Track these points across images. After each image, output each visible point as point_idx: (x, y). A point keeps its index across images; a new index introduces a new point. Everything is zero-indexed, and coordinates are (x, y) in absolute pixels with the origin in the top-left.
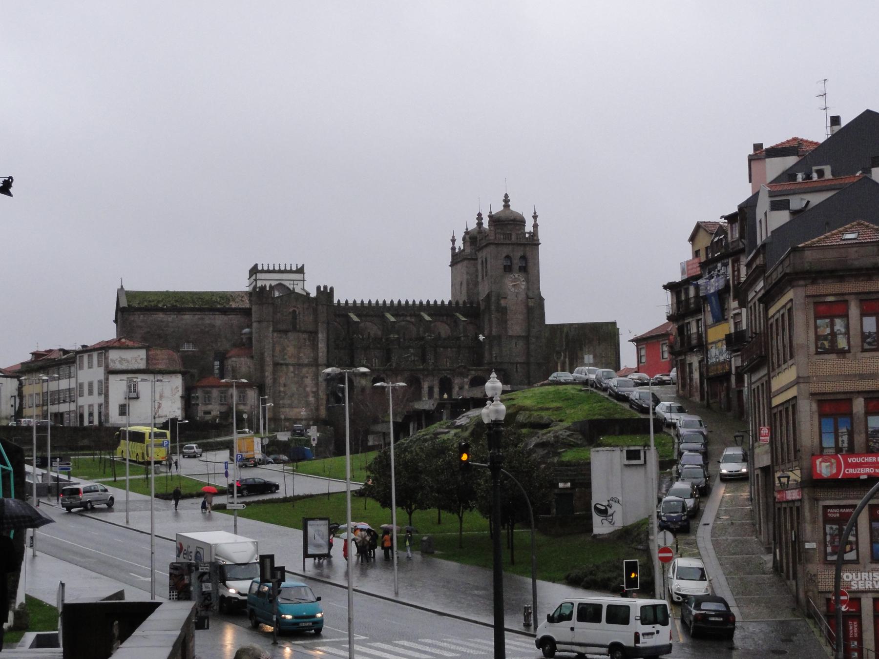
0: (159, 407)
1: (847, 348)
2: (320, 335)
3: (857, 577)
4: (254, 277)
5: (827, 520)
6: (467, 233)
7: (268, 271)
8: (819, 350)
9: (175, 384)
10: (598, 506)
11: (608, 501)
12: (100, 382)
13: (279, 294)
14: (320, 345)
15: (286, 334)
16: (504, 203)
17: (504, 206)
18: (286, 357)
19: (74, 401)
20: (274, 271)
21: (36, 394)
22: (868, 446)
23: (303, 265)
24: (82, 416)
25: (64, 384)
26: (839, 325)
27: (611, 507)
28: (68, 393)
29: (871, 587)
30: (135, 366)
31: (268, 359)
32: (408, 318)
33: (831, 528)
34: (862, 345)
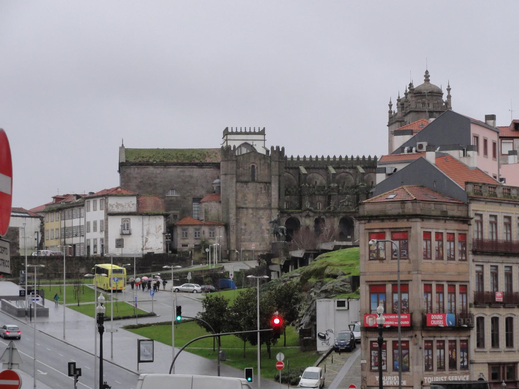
0: (146, 242)
1: (384, 258)
2: (273, 185)
3: (386, 379)
4: (225, 138)
5: (372, 348)
6: (399, 100)
7: (237, 133)
8: (371, 258)
9: (160, 223)
10: (320, 334)
11: (326, 331)
12: (102, 221)
13: (247, 151)
14: (273, 193)
15: (247, 185)
16: (425, 78)
17: (425, 80)
18: (247, 202)
19: (83, 236)
20: (241, 133)
21: (56, 229)
22: (393, 310)
23: (264, 128)
24: (89, 247)
25: (76, 222)
26: (381, 245)
27: (328, 335)
28: (79, 229)
29: (392, 384)
30: (128, 210)
31: (232, 205)
32: (348, 170)
33: (374, 353)
34: (392, 256)
